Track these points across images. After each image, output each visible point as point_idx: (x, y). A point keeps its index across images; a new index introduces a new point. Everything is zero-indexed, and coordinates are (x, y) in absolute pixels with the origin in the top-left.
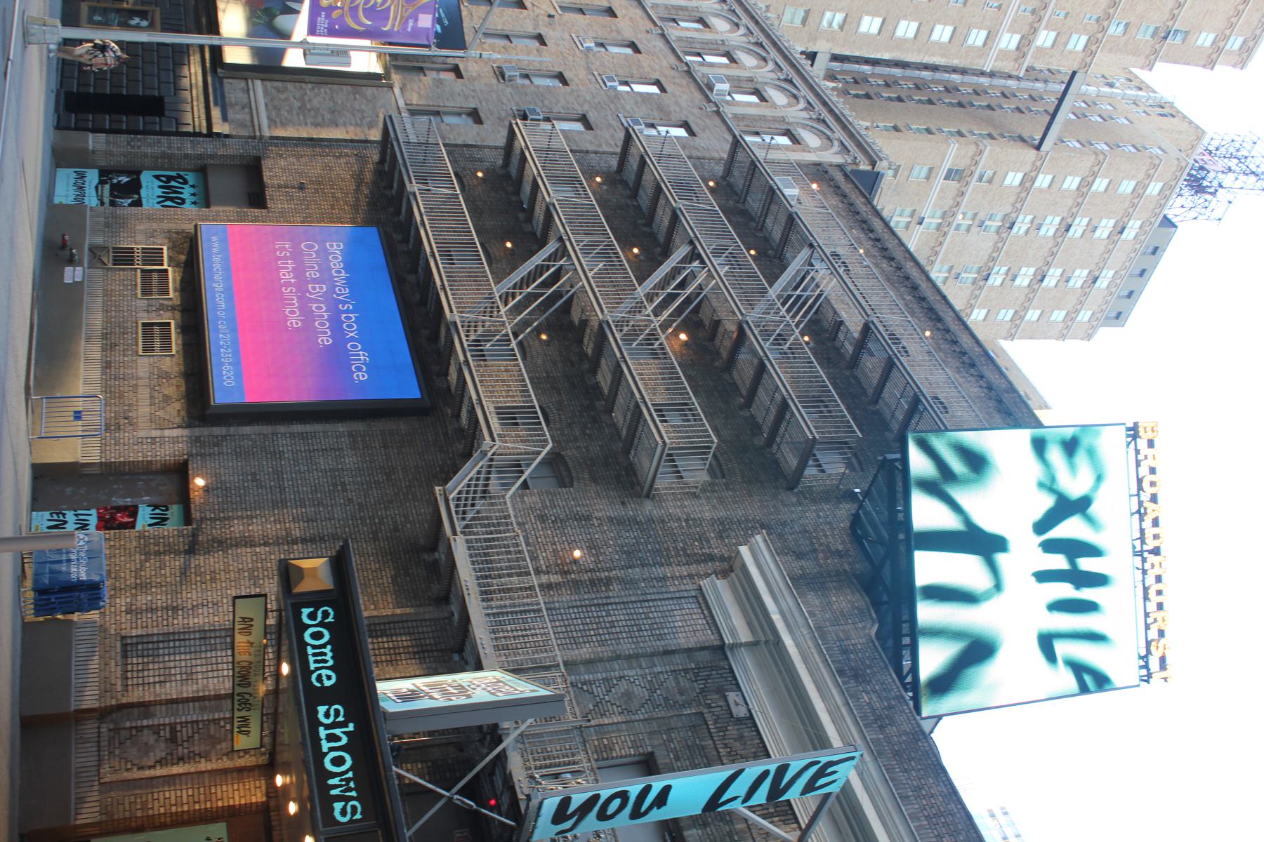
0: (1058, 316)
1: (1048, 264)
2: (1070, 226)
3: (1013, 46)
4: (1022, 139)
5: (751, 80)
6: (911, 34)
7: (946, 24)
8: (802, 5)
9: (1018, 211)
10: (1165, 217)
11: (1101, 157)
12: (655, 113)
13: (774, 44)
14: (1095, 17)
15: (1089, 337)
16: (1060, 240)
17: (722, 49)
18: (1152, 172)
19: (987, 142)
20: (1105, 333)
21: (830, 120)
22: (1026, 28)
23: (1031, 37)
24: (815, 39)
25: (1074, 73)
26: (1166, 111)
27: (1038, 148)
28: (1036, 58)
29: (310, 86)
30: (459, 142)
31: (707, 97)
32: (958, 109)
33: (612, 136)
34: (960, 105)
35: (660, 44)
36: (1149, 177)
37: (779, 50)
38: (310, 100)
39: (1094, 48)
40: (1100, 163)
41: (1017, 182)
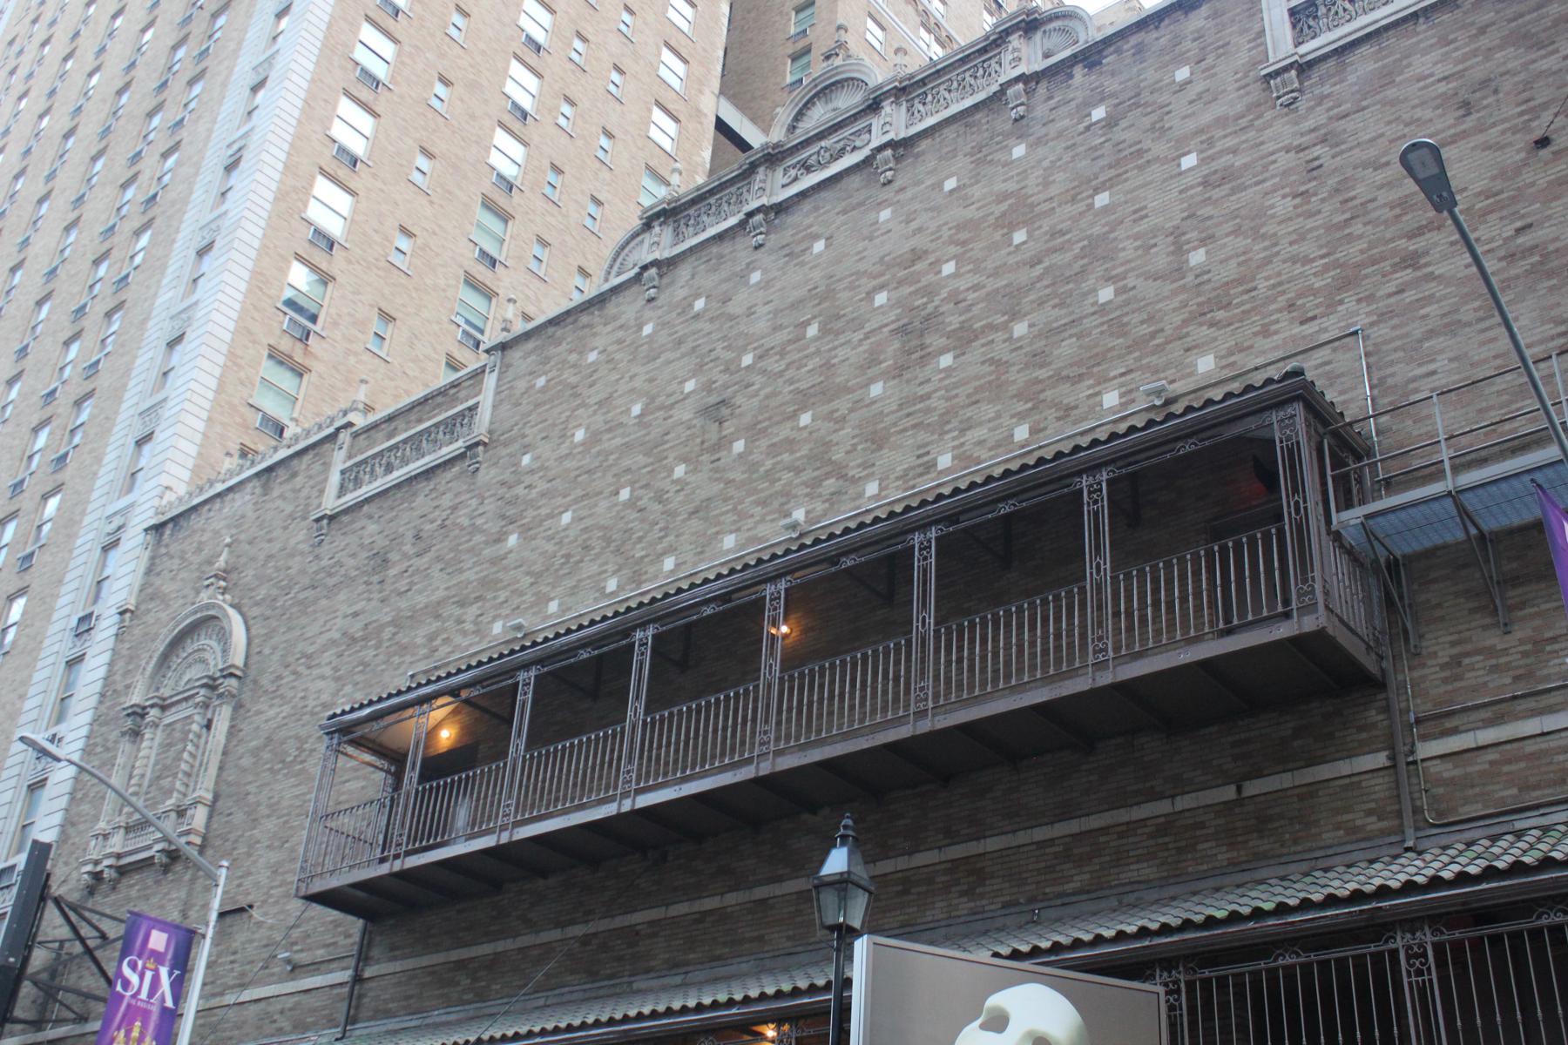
8: (650, 111)
24: (698, 111)
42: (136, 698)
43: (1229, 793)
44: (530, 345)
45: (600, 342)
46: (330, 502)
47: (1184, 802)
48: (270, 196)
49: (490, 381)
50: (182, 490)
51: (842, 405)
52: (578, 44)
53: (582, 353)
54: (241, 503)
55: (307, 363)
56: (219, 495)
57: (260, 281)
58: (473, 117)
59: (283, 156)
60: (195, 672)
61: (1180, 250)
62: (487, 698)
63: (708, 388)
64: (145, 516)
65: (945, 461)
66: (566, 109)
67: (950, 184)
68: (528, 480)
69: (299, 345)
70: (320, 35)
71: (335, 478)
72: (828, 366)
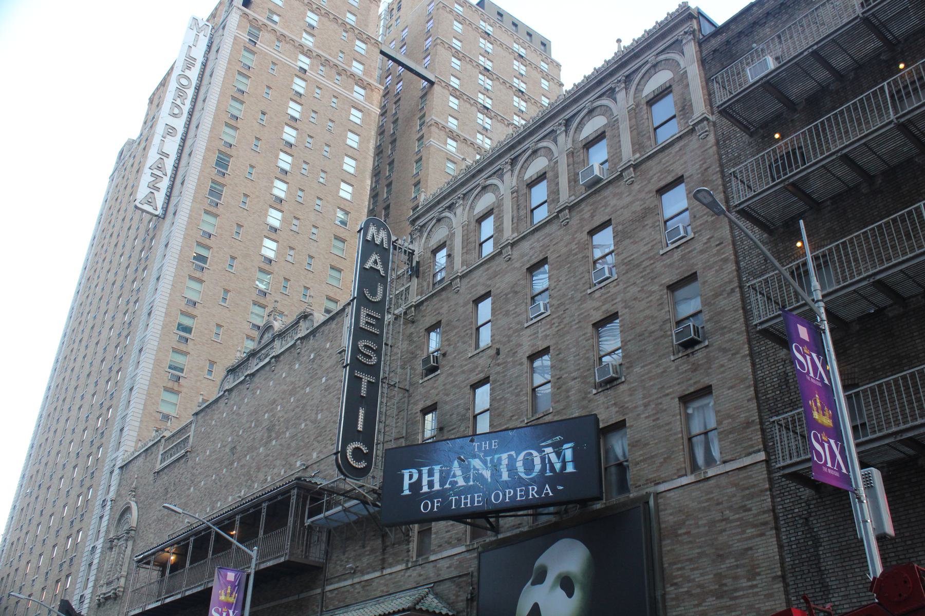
0: (545, 84)
1: (511, 86)
2: (485, 68)
3: (362, 92)
4: (423, 96)
5: (571, 154)
6: (353, 163)
7: (346, 137)
9: (476, 102)
10: (478, 4)
11: (439, 41)
12: (649, 222)
13: (512, 147)
14: (344, 34)
15: (558, 66)
16: (495, 77)
17: (524, 190)
18: (448, 9)
19: (427, 119)
20: (555, 55)
21: (626, 71)
22: (350, 80)
23: (357, 78)
25: (382, 53)
26: (395, 7)
27: (432, 83)
28: (371, 77)
29: (670, 589)
30: (753, 405)
31: (610, 183)
32: (398, 143)
33: (702, 252)
34: (394, 142)
35: (525, 245)
36: (451, 11)
37: (524, 139)
38: (699, 586)
39: (365, 36)
40: (443, 42)
41: (456, 101)
42: (111, 536)
43: (296, 597)
44: (202, 414)
45: (216, 417)
46: (159, 467)
47: (291, 599)
48: (160, 328)
49: (193, 426)
50: (133, 449)
51: (254, 454)
52: (295, 222)
53: (212, 419)
54: (141, 460)
55: (180, 389)
56: (136, 457)
57: (157, 362)
58: (246, 269)
59: (164, 310)
60: (126, 527)
61: (317, 414)
62: (181, 546)
63: (232, 441)
64: (119, 463)
65: (269, 478)
66: (292, 253)
67: (284, 375)
68: (198, 467)
69: (176, 384)
70: (177, 256)
71: (160, 457)
72: (254, 439)
